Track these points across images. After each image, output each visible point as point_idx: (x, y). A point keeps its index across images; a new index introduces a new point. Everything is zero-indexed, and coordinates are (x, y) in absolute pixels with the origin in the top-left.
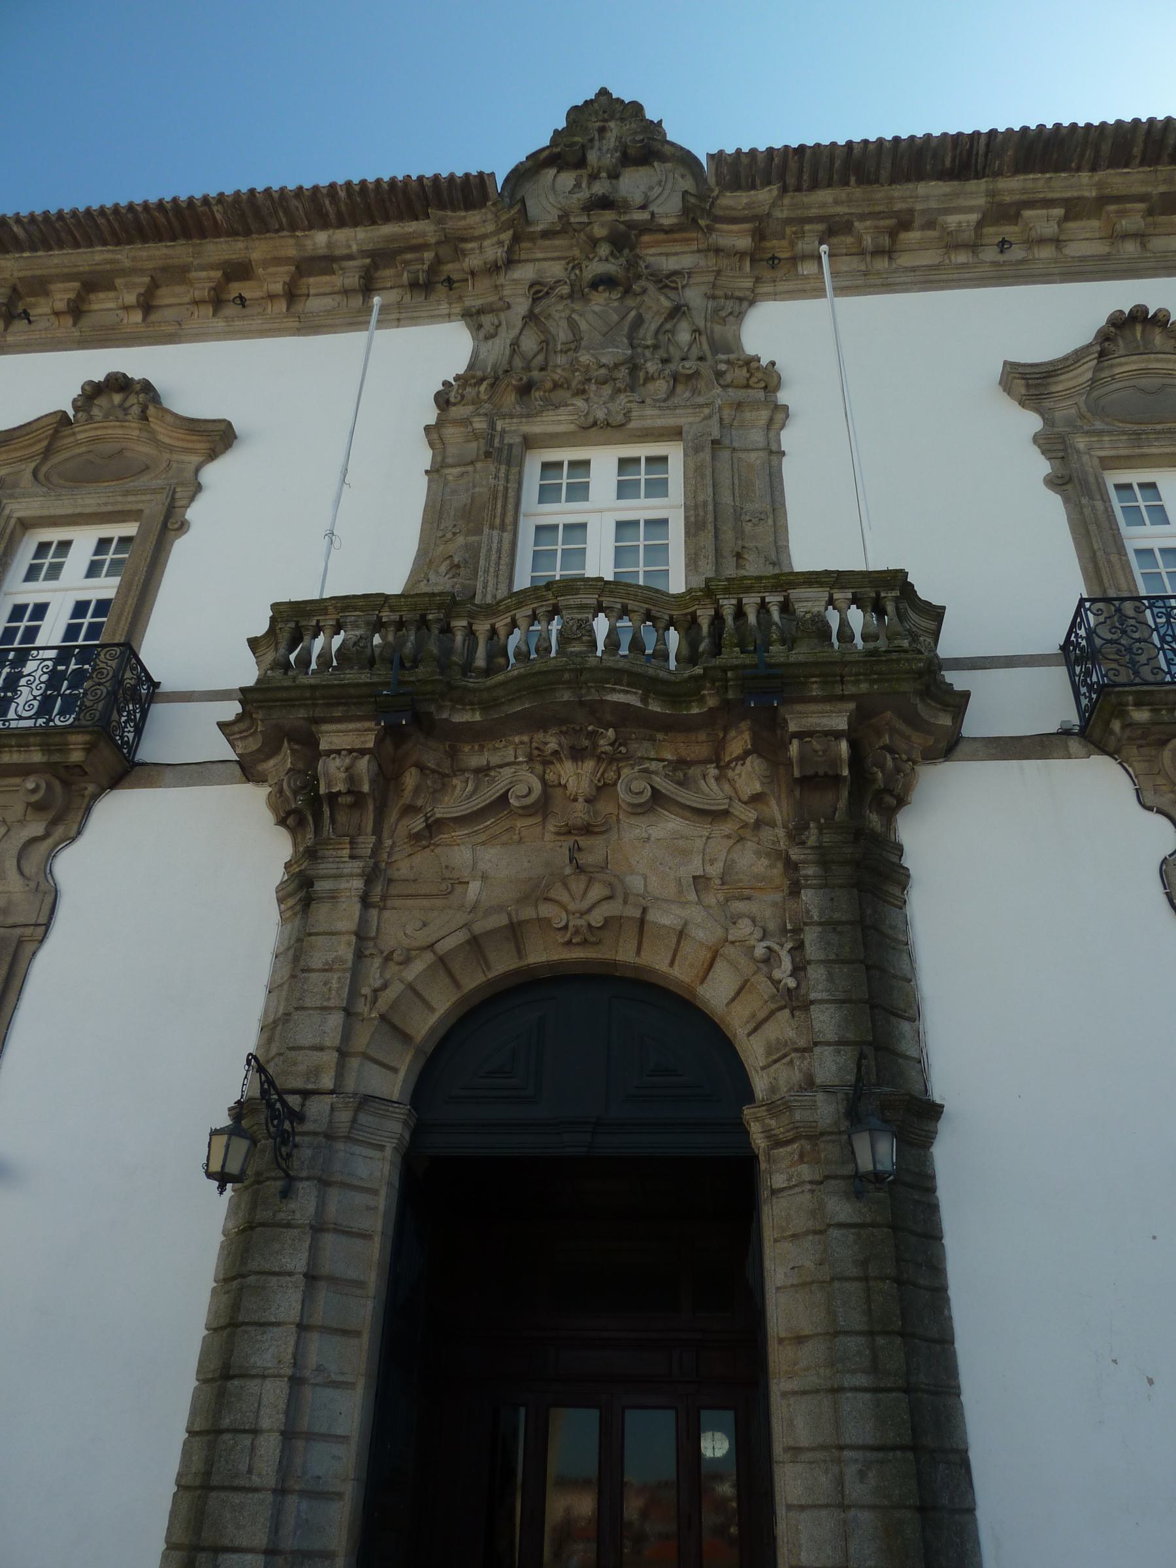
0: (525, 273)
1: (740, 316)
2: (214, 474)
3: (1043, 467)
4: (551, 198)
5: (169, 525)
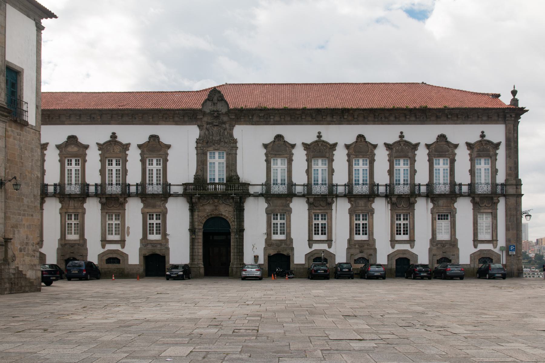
0: (205, 119)
1: (233, 129)
2: (169, 151)
3: (265, 158)
4: (209, 108)
5: (166, 161)
